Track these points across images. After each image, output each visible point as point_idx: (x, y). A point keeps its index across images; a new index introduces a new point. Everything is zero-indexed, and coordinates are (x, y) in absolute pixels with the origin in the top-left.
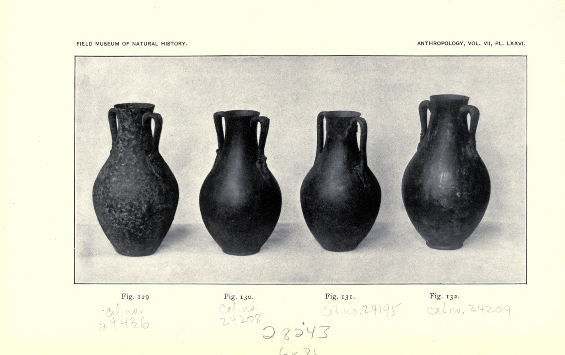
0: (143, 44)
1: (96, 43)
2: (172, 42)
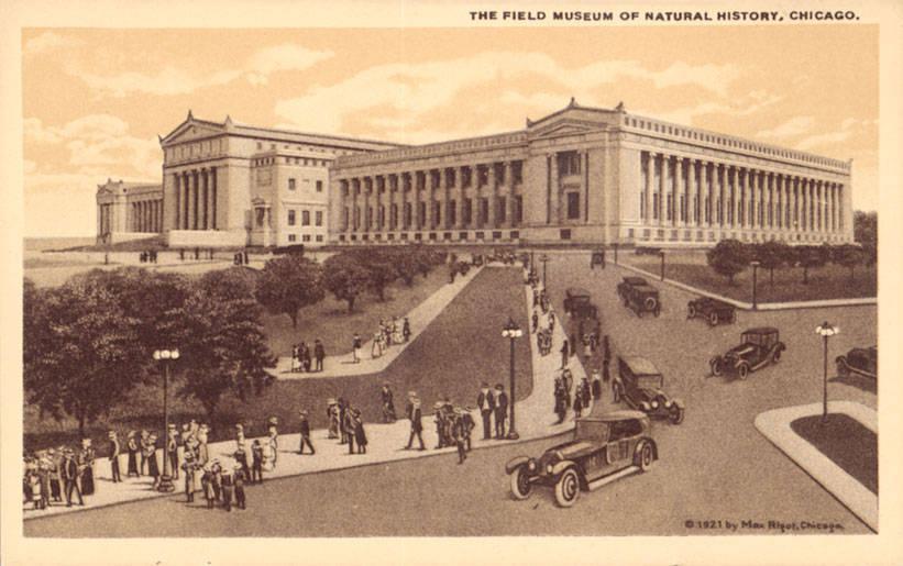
0: (672, 17)
1: (555, 14)
2: (744, 14)
